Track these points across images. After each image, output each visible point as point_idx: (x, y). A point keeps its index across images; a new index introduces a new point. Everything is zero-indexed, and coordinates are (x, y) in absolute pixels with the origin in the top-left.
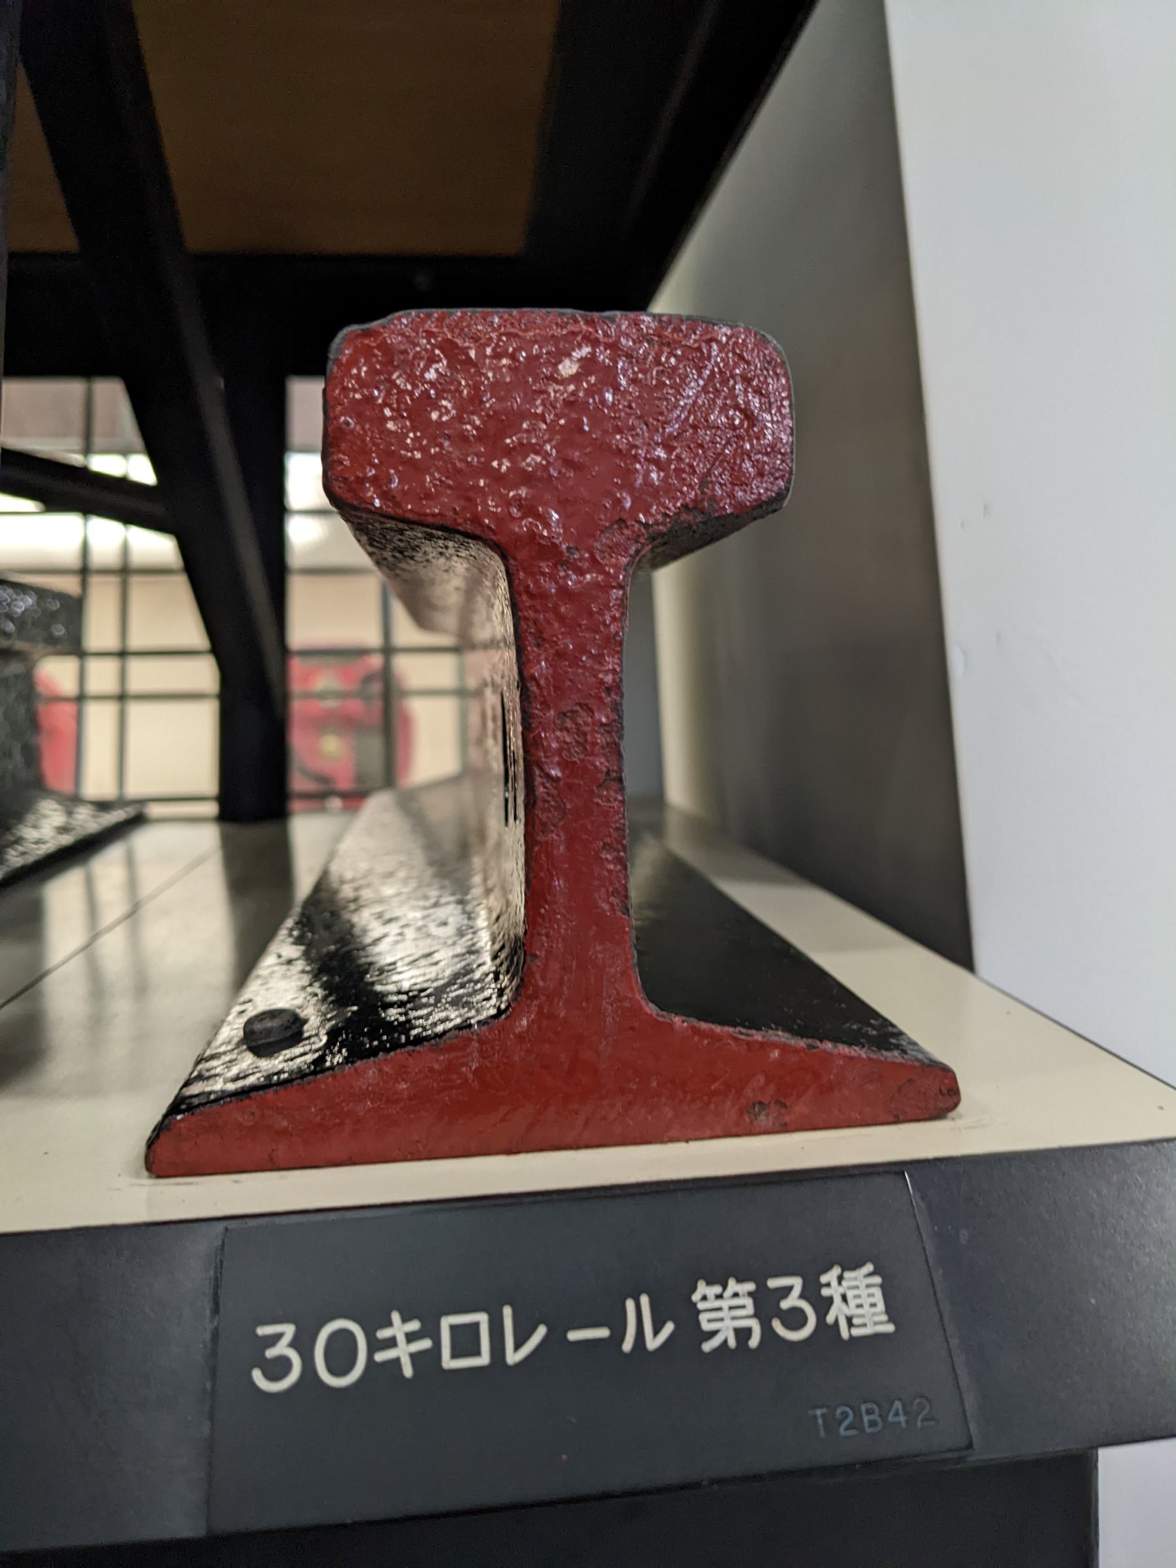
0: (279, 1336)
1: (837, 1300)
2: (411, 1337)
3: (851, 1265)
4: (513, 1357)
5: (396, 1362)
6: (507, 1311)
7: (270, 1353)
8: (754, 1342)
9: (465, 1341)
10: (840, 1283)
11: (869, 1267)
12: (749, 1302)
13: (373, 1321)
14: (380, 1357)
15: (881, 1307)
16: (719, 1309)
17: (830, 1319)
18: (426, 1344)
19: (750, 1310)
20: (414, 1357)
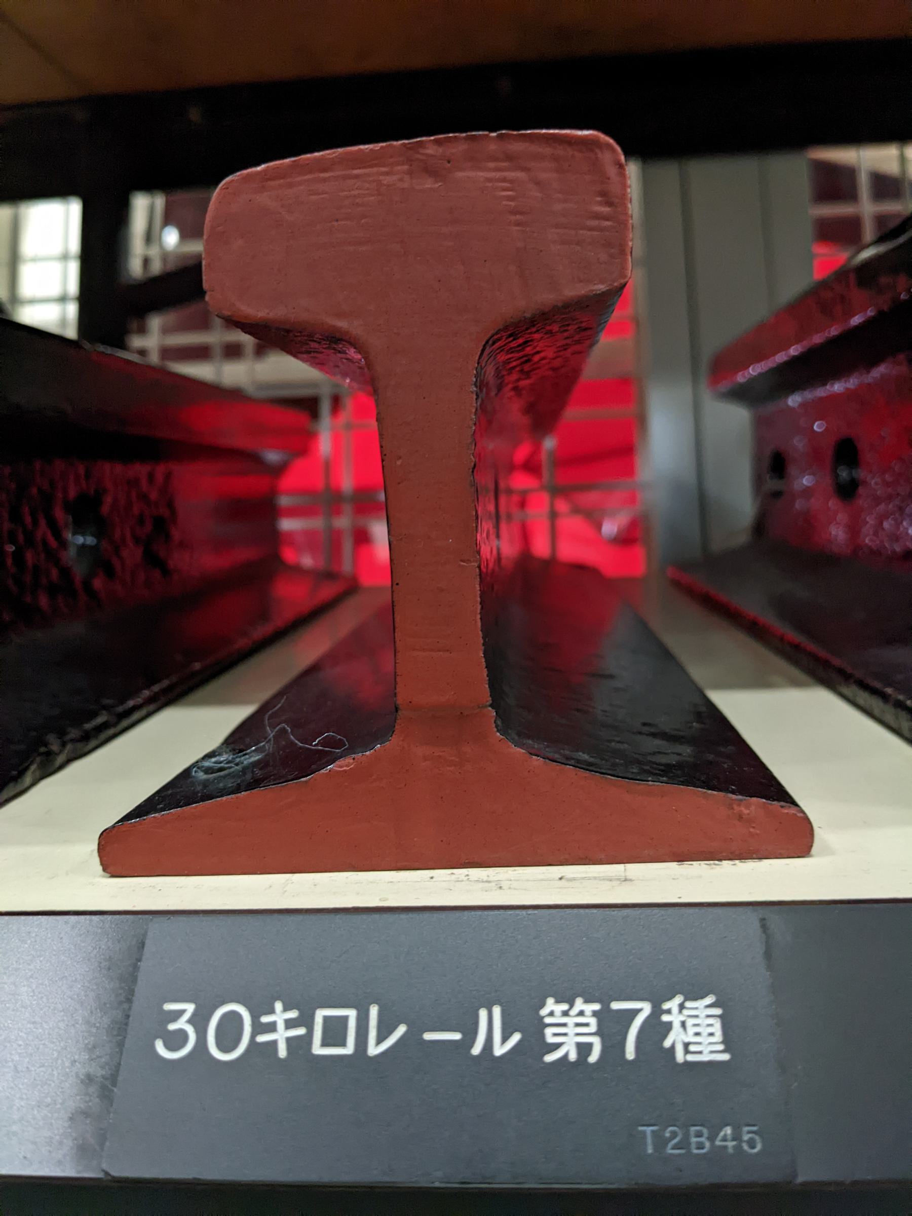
1: (676, 1025)
2: (290, 1024)
4: (373, 1050)
5: (274, 1043)
6: (374, 1011)
7: (172, 1027)
8: (593, 1058)
10: (680, 1012)
11: (709, 1000)
12: (593, 1021)
13: (260, 1008)
14: (261, 1039)
15: (718, 1037)
16: (564, 1025)
17: (667, 1043)
18: (301, 1031)
19: (593, 1028)
20: (289, 1040)
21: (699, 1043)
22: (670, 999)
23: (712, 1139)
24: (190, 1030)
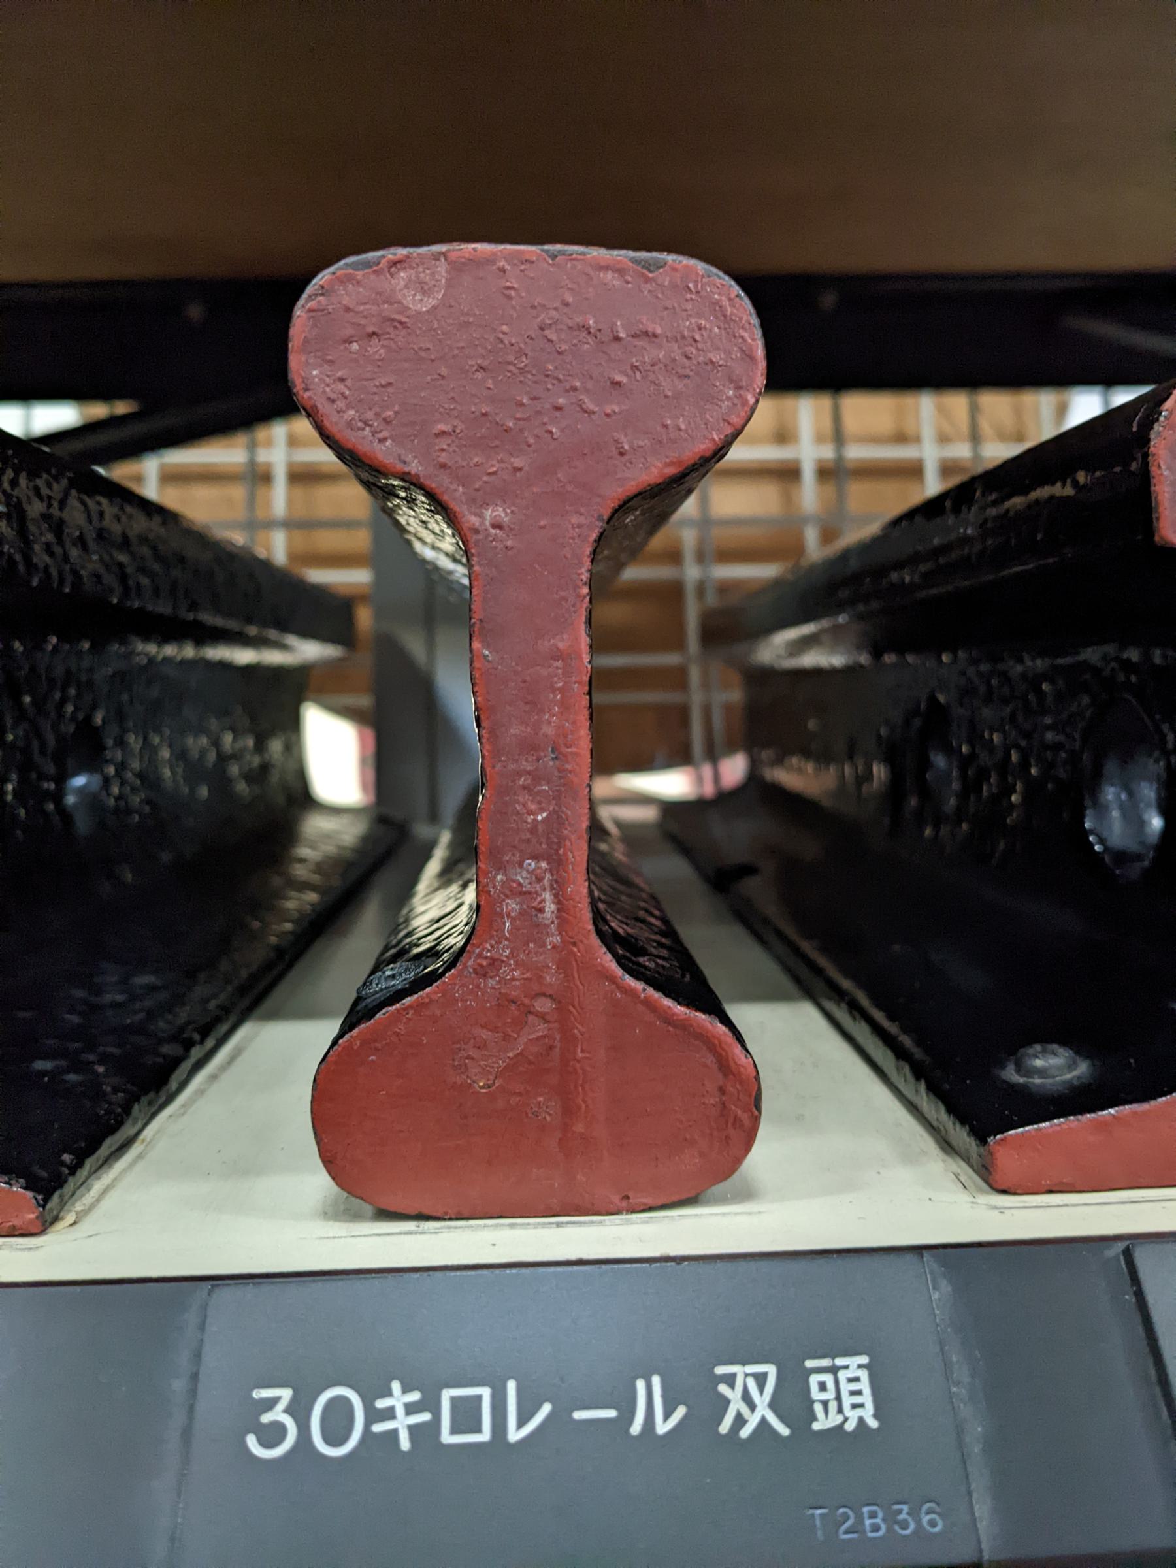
0: (274, 1401)
2: (410, 1409)
5: (393, 1434)
7: (266, 1418)
9: (467, 1415)
13: (373, 1391)
14: (378, 1428)
18: (425, 1417)
20: (412, 1429)
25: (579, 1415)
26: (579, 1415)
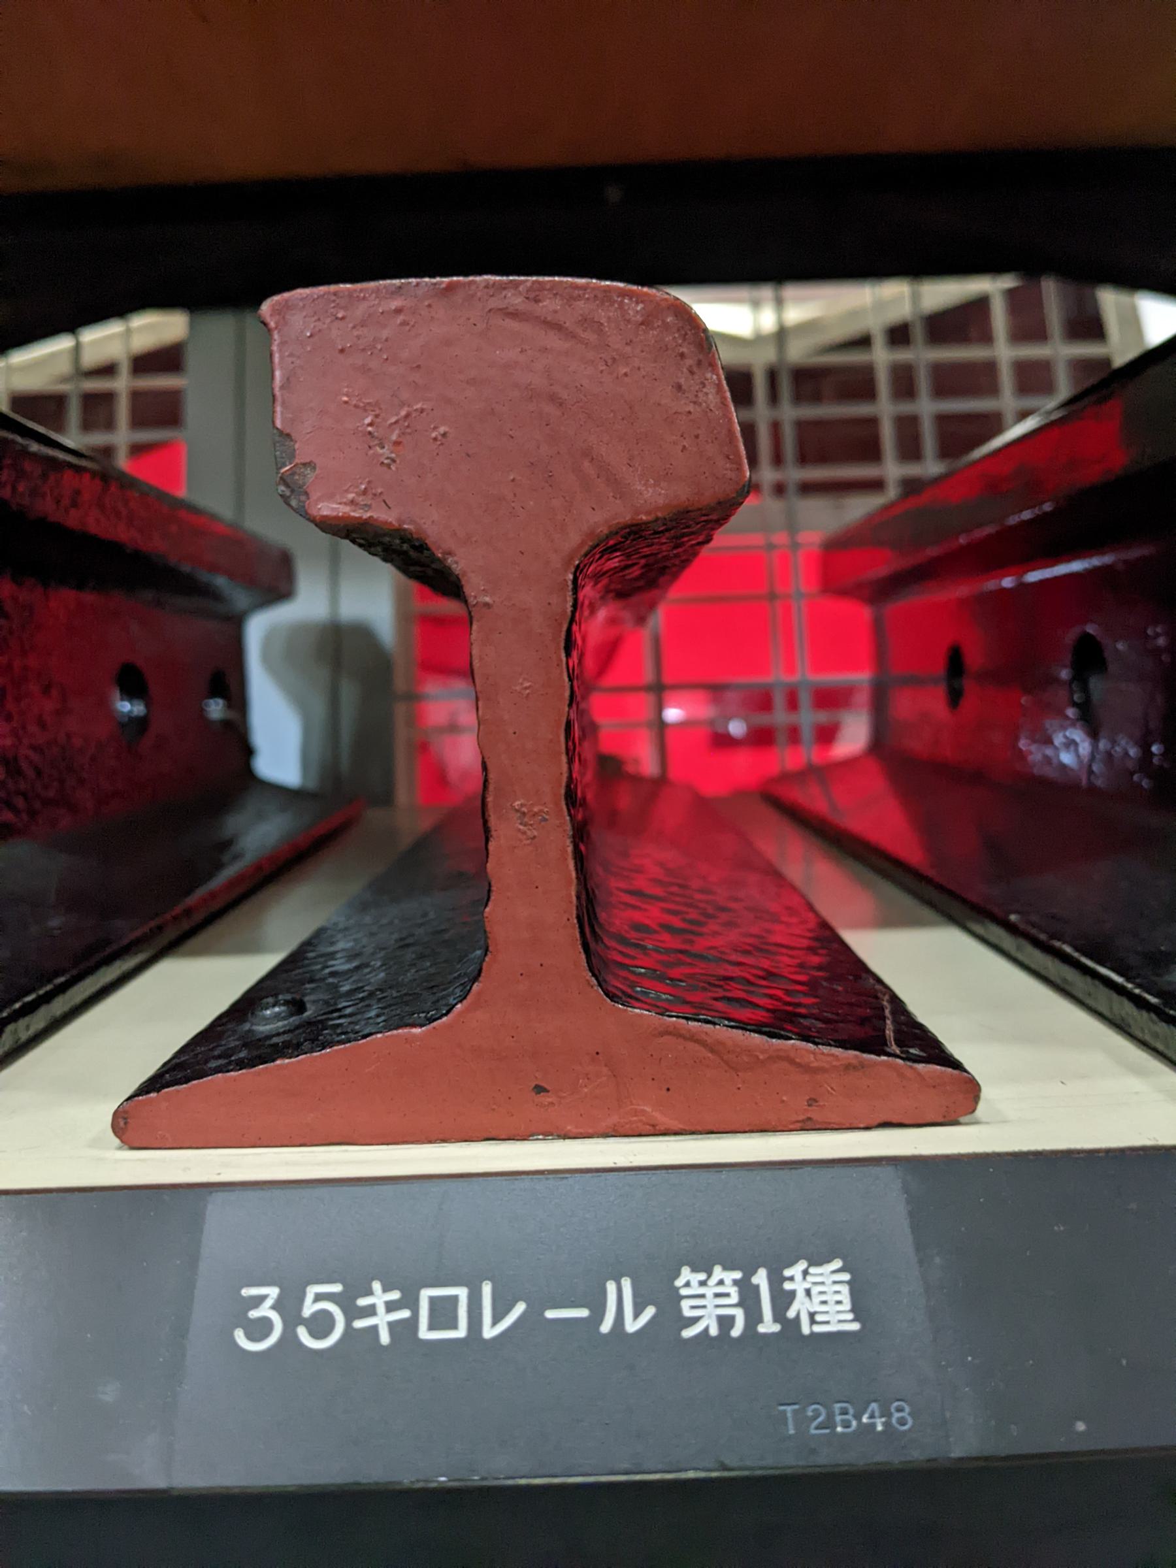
0: (263, 1298)
1: (800, 1294)
2: (391, 1307)
3: (817, 1260)
5: (374, 1329)
7: (254, 1314)
9: (443, 1314)
10: (804, 1278)
11: (837, 1264)
14: (359, 1324)
15: (847, 1305)
18: (405, 1314)
20: (392, 1326)
21: (827, 1312)
22: (791, 1264)
23: (858, 1417)
24: (275, 1317)
25: (550, 1314)
26: (550, 1314)
